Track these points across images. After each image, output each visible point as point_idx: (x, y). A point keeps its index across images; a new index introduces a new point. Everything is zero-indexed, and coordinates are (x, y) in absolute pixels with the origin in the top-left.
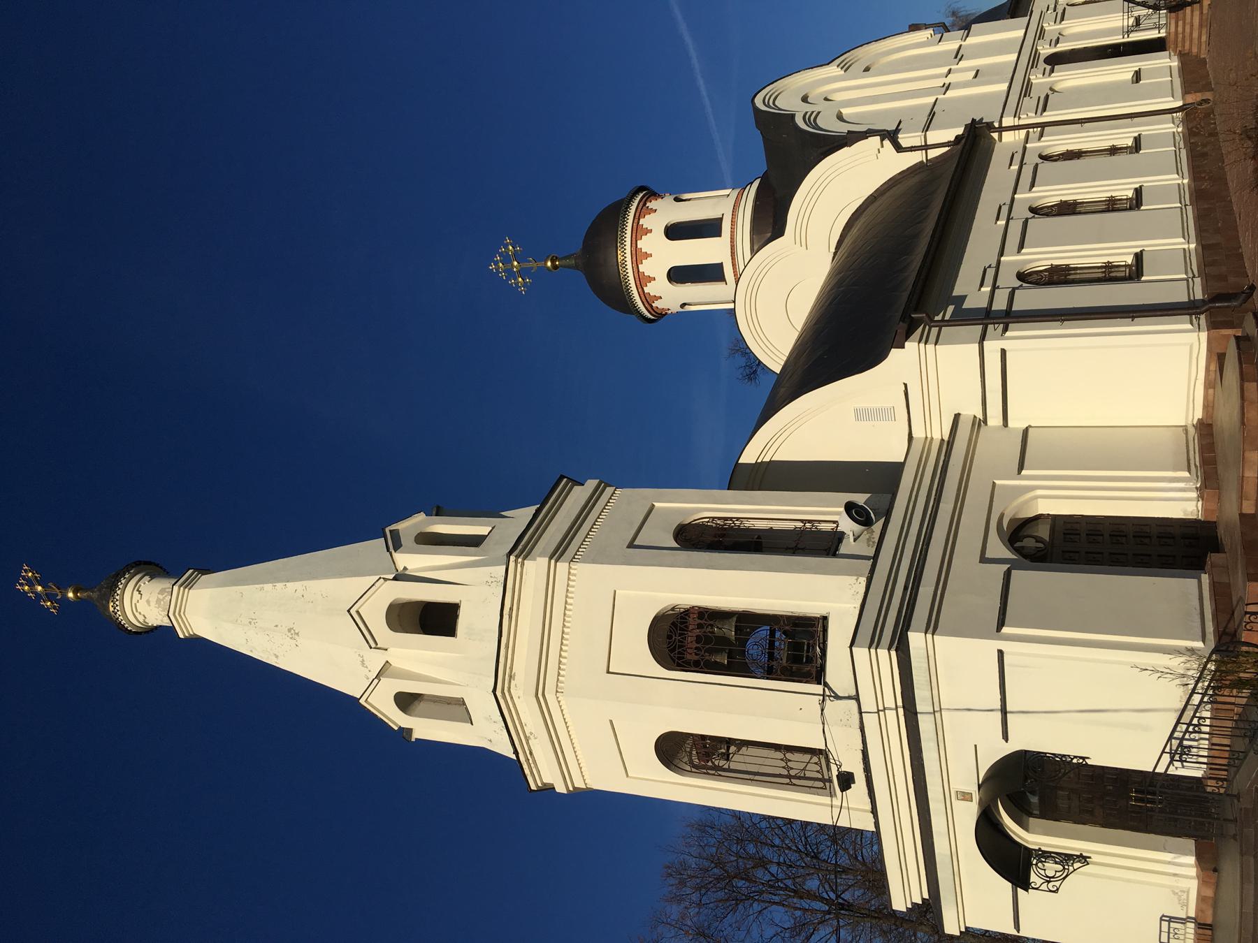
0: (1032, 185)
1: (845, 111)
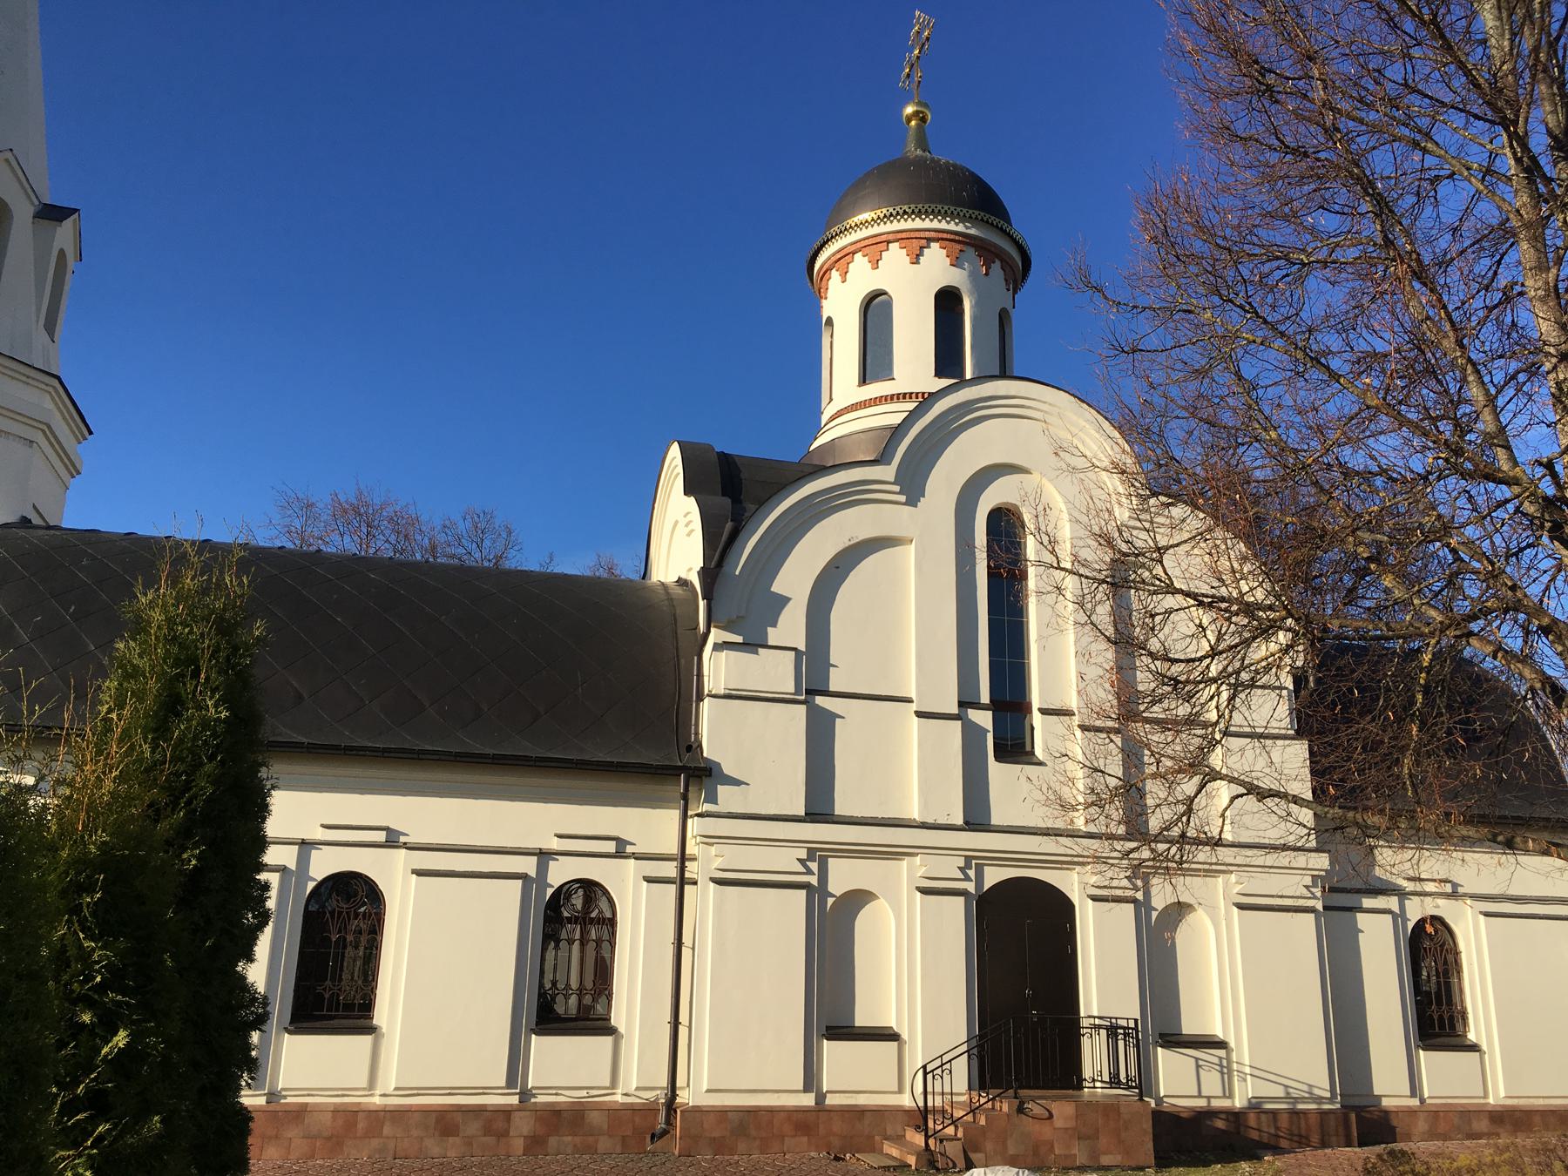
0: (419, 873)
1: (913, 546)
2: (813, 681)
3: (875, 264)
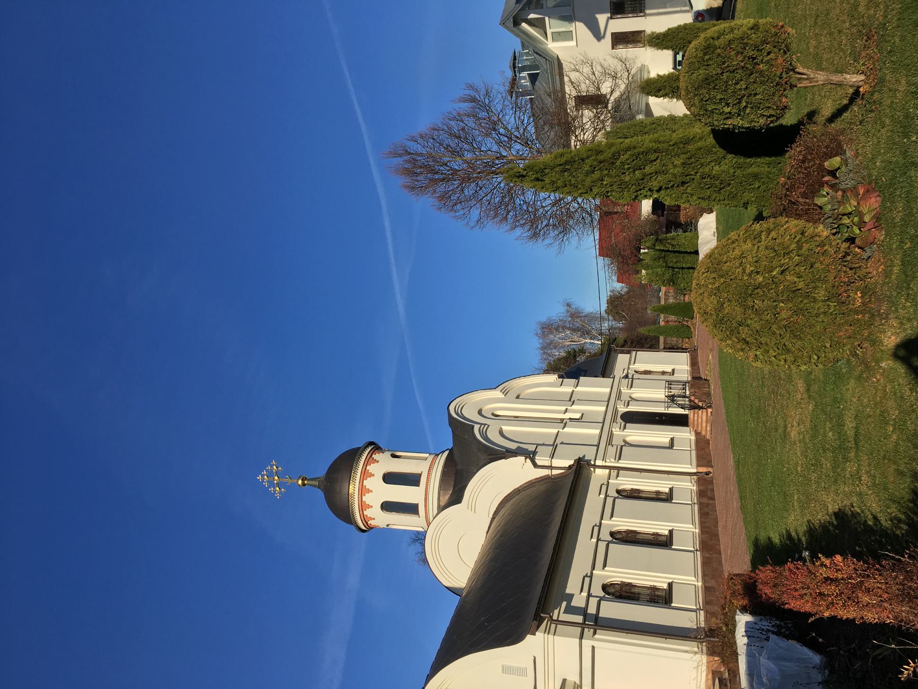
0: (612, 516)
1: (505, 428)
3: (372, 475)
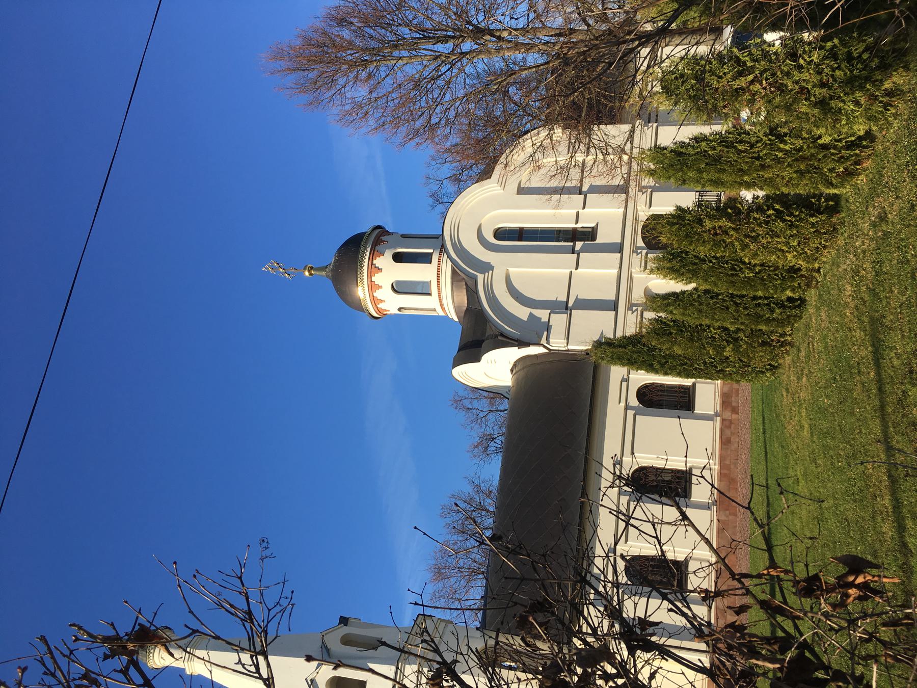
1: (511, 270)
2: (564, 307)
3: (380, 287)
